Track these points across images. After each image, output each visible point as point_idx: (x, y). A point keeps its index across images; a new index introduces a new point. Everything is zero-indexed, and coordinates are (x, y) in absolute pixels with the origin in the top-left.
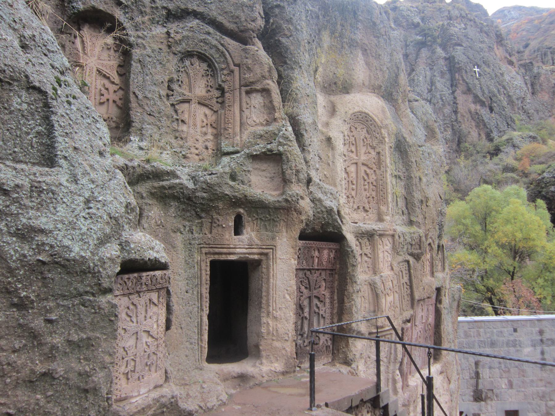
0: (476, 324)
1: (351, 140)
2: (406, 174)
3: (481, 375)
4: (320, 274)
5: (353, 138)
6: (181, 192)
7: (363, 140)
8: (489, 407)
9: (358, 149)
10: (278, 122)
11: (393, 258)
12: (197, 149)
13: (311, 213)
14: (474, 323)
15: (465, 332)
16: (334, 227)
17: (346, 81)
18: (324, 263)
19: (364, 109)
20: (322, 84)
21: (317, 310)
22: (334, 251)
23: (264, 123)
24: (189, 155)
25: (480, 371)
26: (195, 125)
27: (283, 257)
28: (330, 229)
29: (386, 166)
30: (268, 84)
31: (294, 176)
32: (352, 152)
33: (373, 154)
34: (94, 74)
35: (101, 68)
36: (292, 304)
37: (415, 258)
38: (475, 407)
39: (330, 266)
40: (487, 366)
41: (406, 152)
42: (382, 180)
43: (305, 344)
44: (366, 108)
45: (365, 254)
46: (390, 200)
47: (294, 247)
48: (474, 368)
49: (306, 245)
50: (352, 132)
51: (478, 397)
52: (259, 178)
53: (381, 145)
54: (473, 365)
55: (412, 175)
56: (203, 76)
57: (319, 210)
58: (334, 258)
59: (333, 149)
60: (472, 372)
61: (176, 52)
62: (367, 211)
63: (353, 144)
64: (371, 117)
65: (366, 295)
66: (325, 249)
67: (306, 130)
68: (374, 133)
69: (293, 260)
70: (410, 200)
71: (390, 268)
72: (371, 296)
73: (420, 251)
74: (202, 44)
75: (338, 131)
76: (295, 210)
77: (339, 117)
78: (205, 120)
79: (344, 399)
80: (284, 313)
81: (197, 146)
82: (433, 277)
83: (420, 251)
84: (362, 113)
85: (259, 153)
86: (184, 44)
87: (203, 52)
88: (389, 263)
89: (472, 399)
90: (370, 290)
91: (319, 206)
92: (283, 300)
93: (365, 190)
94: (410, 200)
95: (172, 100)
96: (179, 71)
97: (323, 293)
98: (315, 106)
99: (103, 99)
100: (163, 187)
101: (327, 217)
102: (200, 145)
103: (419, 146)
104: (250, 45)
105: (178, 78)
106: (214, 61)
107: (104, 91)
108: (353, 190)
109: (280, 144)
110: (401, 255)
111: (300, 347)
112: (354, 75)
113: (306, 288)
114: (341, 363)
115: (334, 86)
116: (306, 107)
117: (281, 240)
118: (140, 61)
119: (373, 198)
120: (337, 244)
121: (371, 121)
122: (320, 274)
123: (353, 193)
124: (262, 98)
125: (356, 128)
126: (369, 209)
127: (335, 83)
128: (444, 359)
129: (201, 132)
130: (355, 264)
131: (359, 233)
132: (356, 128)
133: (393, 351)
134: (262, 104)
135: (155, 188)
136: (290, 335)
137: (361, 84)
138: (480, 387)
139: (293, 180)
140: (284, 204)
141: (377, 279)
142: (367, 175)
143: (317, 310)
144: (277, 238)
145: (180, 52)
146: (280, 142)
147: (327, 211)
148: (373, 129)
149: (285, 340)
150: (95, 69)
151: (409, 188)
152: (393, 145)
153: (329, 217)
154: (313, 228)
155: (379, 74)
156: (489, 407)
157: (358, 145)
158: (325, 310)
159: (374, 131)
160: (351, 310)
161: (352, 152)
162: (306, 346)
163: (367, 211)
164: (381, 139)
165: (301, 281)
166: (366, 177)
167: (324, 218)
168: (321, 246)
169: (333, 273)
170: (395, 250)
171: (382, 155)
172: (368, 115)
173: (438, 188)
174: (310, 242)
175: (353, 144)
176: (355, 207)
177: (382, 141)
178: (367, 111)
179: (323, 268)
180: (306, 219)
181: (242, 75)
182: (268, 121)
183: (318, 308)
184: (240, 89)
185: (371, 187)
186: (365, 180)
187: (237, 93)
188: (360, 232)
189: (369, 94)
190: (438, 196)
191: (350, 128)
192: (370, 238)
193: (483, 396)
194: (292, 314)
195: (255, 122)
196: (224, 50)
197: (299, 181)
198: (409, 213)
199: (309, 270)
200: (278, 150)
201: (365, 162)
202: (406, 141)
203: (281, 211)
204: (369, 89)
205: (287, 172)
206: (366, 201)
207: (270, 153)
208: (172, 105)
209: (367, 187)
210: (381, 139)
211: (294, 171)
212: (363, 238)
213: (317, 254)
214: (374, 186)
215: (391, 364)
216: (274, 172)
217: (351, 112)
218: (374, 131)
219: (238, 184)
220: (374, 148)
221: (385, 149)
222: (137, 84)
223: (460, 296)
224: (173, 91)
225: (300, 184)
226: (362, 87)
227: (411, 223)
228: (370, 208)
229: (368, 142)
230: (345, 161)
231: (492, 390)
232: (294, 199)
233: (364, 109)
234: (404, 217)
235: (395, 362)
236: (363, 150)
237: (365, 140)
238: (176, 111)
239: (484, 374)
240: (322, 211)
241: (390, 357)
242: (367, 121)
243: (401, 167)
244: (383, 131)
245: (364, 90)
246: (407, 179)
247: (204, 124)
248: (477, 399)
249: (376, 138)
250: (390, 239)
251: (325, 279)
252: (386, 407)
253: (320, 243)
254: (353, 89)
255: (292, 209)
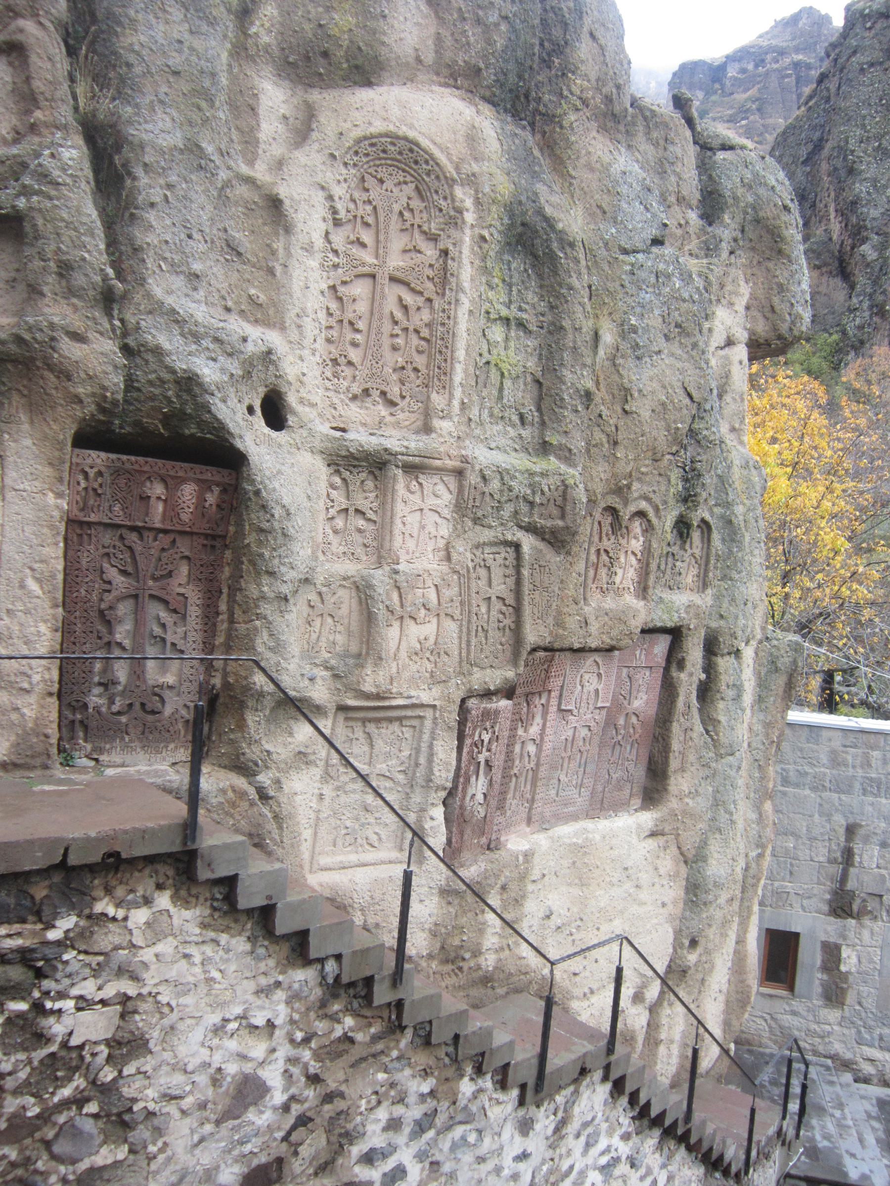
0: (865, 736)
1: (360, 212)
2: (549, 317)
3: (857, 859)
4: (174, 541)
5: (369, 208)
7: (401, 214)
8: (866, 934)
9: (381, 238)
10: (39, 134)
11: (459, 532)
13: (116, 380)
14: (860, 735)
15: (833, 752)
16: (201, 424)
17: (359, 48)
18: (185, 517)
19: (404, 128)
20: (276, 52)
21: (157, 630)
22: (216, 490)
23: (9, 137)
25: (857, 847)
27: (21, 487)
28: (191, 430)
29: (460, 289)
30: (21, 31)
31: (51, 279)
32: (363, 245)
33: (430, 252)
36: (47, 604)
37: (543, 539)
38: (829, 928)
39: (203, 526)
40: (875, 839)
41: (552, 258)
42: (443, 324)
43: (115, 708)
44: (411, 126)
45: (357, 511)
46: (459, 376)
47: (56, 462)
48: (843, 839)
49: (118, 464)
50: (367, 190)
51: (842, 905)
53: (452, 232)
54: (842, 831)
55: (567, 323)
57: (152, 377)
58: (218, 506)
59: (288, 230)
60: (834, 847)
62: (392, 404)
63: (367, 225)
64: (426, 152)
65: (344, 611)
66: (184, 480)
67: (146, 165)
68: (435, 197)
69: (51, 495)
70: (549, 389)
71: (442, 553)
72: (355, 616)
73: (560, 523)
75: (311, 185)
76: (50, 367)
77: (316, 146)
79: (31, 842)
80: (21, 625)
82: (644, 598)
83: (560, 523)
84: (398, 137)
88: (441, 543)
89: (826, 908)
90: (355, 602)
91: (153, 366)
92: (19, 592)
93: (395, 348)
94: (549, 389)
97: (182, 590)
98: (204, 104)
101: (178, 396)
103: (625, 252)
108: (355, 344)
109: (26, 191)
110: (490, 527)
111: (99, 713)
112: (385, 34)
113: (124, 573)
114: (225, 767)
115: (321, 61)
116: (161, 102)
117: (15, 441)
119: (416, 370)
120: (225, 472)
121: (427, 162)
122: (174, 541)
123: (354, 355)
124: (11, 69)
125: (381, 181)
126: (397, 400)
127: (325, 54)
128: (673, 804)
130: (265, 525)
131: (338, 455)
132: (381, 181)
133: (422, 760)
134: (9, 87)
136: (36, 678)
137: (411, 60)
138: (851, 885)
139: (46, 289)
140: (13, 348)
141: (380, 578)
142: (405, 308)
143: (157, 630)
144: (6, 436)
146: (24, 187)
147: (177, 382)
148: (434, 184)
149: (21, 689)
151: (550, 357)
152: (494, 235)
153: (185, 396)
154: (137, 424)
155: (473, 33)
156: (866, 934)
157: (381, 226)
158: (188, 633)
159: (437, 192)
160: (252, 641)
161: (363, 245)
162: (119, 713)
163: (392, 404)
164: (452, 213)
165: (107, 554)
166: (399, 315)
167: (168, 399)
168: (172, 473)
169: (218, 544)
170: (467, 510)
171: (453, 259)
172: (417, 145)
173: (682, 371)
174: (133, 458)
175: (367, 225)
176: (356, 389)
177: (455, 220)
178: (411, 134)
179: (179, 528)
180: (94, 395)
182: (18, 133)
183: (163, 626)
185: (415, 341)
186: (396, 323)
188: (344, 453)
189: (436, 88)
190: (680, 391)
191: (363, 179)
192: (377, 472)
193: (855, 907)
194: (43, 628)
197: (71, 292)
198: (543, 423)
199: (133, 529)
200: (13, 207)
201: (399, 274)
202: (552, 227)
203: (9, 366)
204: (438, 74)
205: (30, 265)
206: (395, 377)
209: (400, 341)
210: (452, 213)
211: (52, 264)
212: (355, 471)
213: (158, 489)
214: (424, 339)
215: (418, 790)
216: (16, 266)
217: (357, 133)
218: (437, 192)
220: (433, 238)
221: (462, 241)
223: (795, 662)
225: (75, 300)
226: (411, 71)
227: (544, 448)
228: (403, 397)
229: (417, 221)
230: (336, 266)
231: (881, 896)
232: (38, 335)
233: (404, 128)
234: (526, 433)
235: (429, 787)
236: (397, 242)
237: (407, 214)
239: (865, 857)
240: (160, 379)
241: (414, 773)
242: (416, 162)
243: (531, 297)
244: (459, 192)
245: (421, 77)
246: (550, 332)
248: (839, 911)
249: (441, 210)
250: (452, 481)
251: (187, 558)
252: (230, 883)
253: (169, 464)
254: (385, 74)
255: (39, 363)
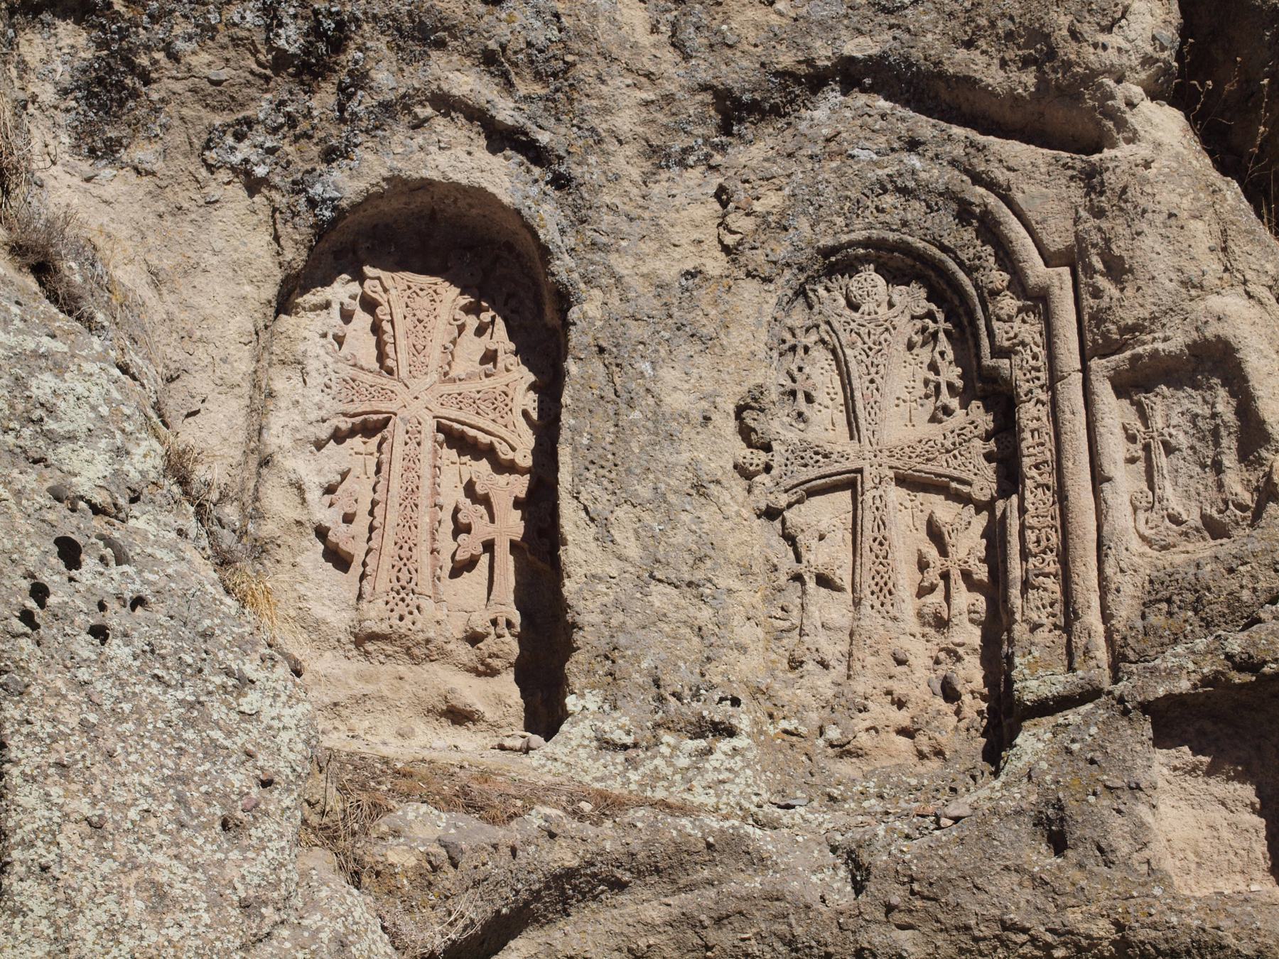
6: (781, 938)
12: (900, 704)
24: (864, 740)
26: (885, 590)
34: (428, 444)
35: (454, 414)
52: (1218, 815)
56: (910, 346)
61: (766, 270)
74: (889, 200)
78: (932, 553)
81: (899, 688)
85: (1184, 685)
86: (804, 224)
87: (891, 236)
95: (766, 491)
96: (793, 349)
99: (470, 545)
100: (688, 920)
102: (919, 682)
104: (1113, 145)
105: (789, 384)
106: (953, 266)
107: (472, 512)
118: (601, 350)
129: (920, 615)
135: (651, 927)
145: (788, 265)
150: (429, 425)
181: (1088, 301)
184: (1085, 370)
187: (1072, 392)
195: (1175, 520)
196: (992, 200)
207: (1249, 678)
208: (771, 514)
219: (1081, 866)
222: (591, 457)
224: (767, 448)
238: (790, 539)
247: (933, 576)
